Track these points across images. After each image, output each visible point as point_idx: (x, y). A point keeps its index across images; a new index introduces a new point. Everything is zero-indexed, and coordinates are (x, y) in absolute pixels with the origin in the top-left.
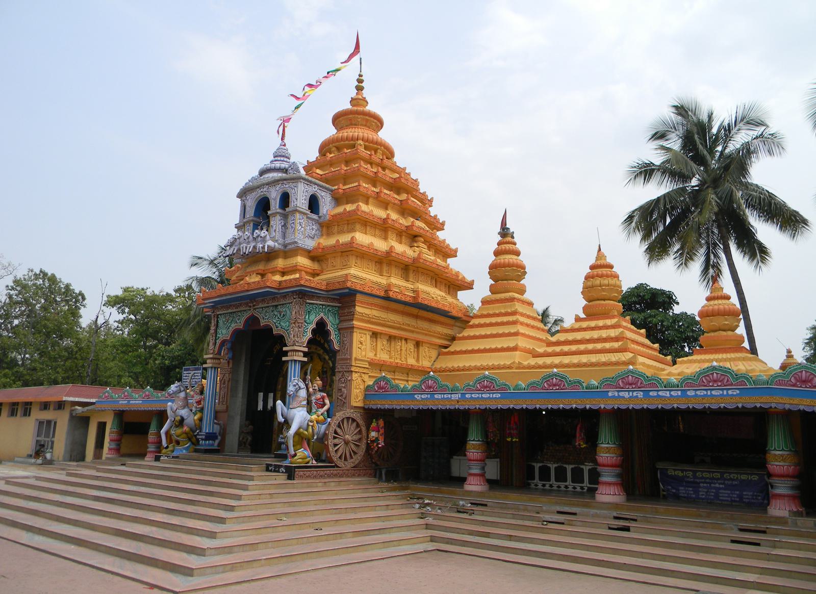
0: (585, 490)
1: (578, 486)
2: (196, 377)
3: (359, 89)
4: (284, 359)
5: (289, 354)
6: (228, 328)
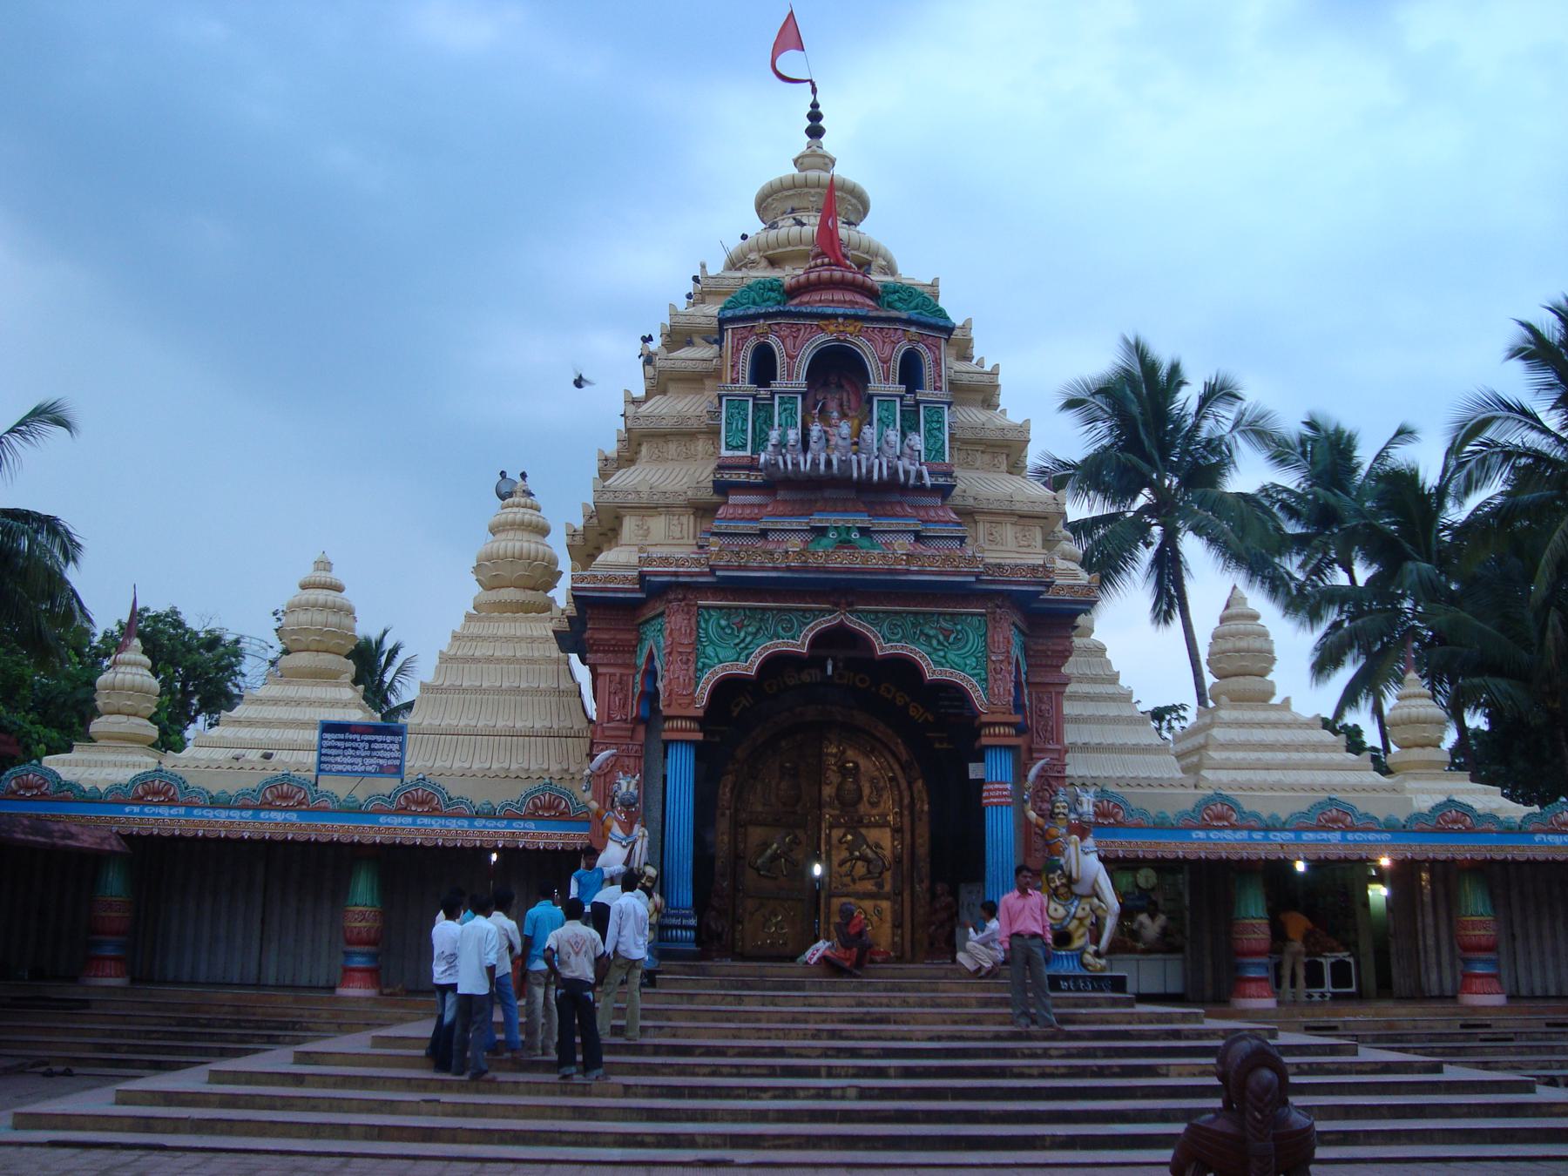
0: (1327, 999)
1: (1316, 992)
2: (381, 753)
3: (815, 132)
4: (984, 741)
5: (983, 732)
6: (746, 648)
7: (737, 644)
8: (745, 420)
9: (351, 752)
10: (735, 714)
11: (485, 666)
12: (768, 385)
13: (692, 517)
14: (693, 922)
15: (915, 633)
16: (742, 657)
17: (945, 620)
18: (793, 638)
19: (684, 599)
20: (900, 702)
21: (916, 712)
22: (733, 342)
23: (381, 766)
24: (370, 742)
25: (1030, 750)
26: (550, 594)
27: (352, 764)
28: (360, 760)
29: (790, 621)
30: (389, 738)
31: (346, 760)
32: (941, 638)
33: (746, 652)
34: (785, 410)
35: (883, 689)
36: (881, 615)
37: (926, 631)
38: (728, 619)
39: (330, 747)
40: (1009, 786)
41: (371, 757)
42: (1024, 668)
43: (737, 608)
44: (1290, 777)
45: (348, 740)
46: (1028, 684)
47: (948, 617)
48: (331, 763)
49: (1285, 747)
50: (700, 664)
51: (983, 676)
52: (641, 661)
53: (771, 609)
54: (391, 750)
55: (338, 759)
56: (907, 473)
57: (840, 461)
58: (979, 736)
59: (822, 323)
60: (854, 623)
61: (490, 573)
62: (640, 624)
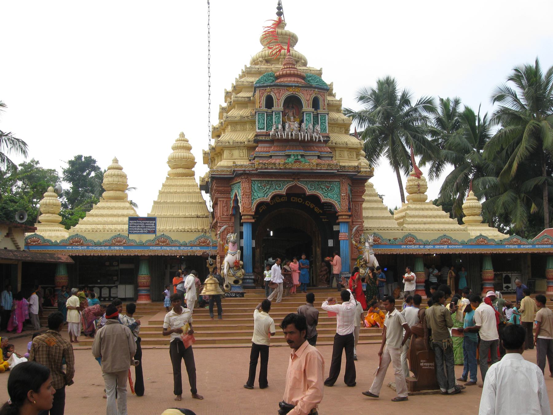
2: (149, 227)
3: (280, 14)
5: (339, 218)
6: (266, 193)
7: (264, 192)
8: (264, 120)
9: (139, 226)
10: (260, 212)
11: (174, 195)
12: (271, 108)
13: (246, 150)
14: (253, 277)
15: (318, 187)
16: (265, 196)
17: (327, 183)
18: (281, 190)
19: (247, 178)
20: (312, 207)
21: (316, 210)
22: (259, 94)
23: (149, 231)
24: (145, 223)
25: (353, 222)
26: (193, 169)
27: (139, 230)
28: (142, 229)
29: (280, 184)
30: (151, 222)
31: (137, 229)
32: (326, 189)
33: (267, 194)
34: (276, 117)
35: (306, 203)
36: (307, 182)
37: (322, 187)
38: (261, 184)
39: (132, 225)
40: (347, 234)
41: (145, 228)
42: (351, 197)
43: (263, 181)
44: (432, 226)
45: (138, 223)
46: (352, 201)
47: (328, 182)
48: (132, 230)
49: (430, 217)
50: (252, 198)
51: (339, 200)
52: (233, 196)
53: (274, 181)
54: (152, 226)
55: (135, 229)
56: (316, 138)
57: (295, 134)
58: (338, 219)
59: (288, 88)
60: (299, 184)
61: (174, 163)
62: (231, 185)
